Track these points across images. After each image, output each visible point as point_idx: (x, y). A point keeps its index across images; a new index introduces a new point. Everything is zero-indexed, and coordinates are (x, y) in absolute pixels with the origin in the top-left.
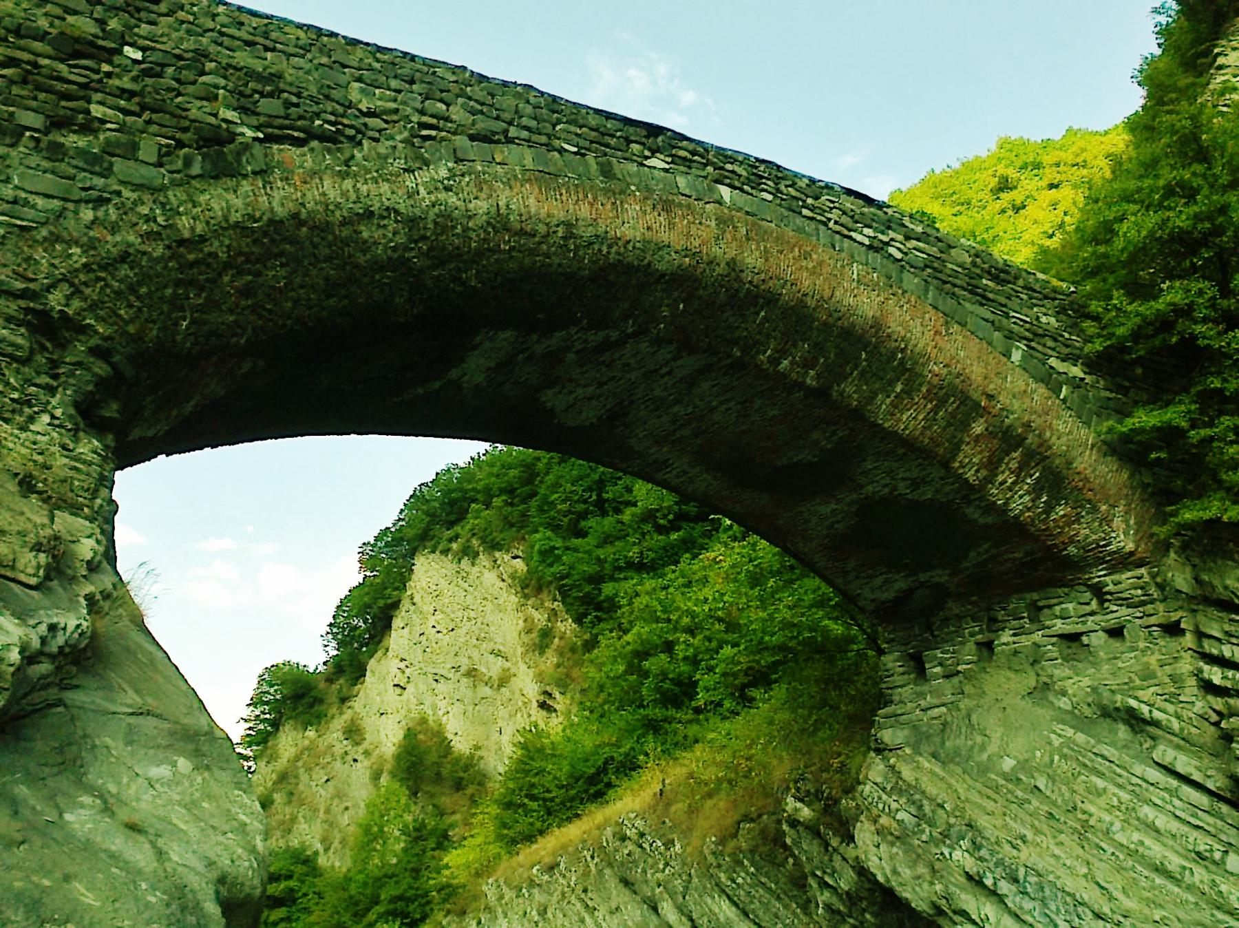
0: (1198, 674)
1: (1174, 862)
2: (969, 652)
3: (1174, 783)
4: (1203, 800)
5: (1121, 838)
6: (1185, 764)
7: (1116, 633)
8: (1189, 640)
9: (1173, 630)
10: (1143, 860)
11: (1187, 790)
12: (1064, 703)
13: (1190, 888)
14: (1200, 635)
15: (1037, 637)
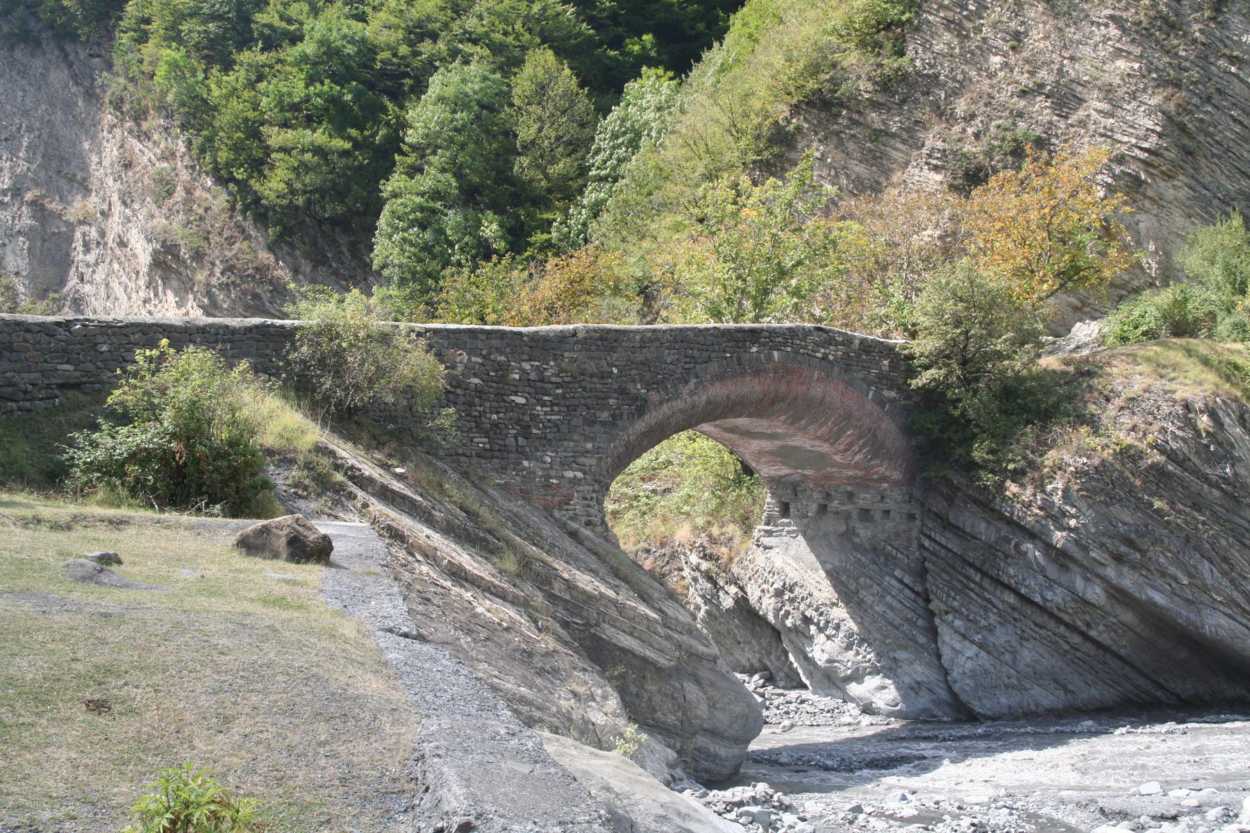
0: (919, 539)
1: (897, 621)
2: (814, 507)
3: (902, 587)
4: (913, 596)
5: (877, 608)
6: (907, 580)
7: (887, 512)
8: (918, 523)
9: (911, 517)
10: (885, 619)
11: (907, 592)
12: (857, 540)
13: (902, 632)
14: (924, 525)
15: (849, 507)
